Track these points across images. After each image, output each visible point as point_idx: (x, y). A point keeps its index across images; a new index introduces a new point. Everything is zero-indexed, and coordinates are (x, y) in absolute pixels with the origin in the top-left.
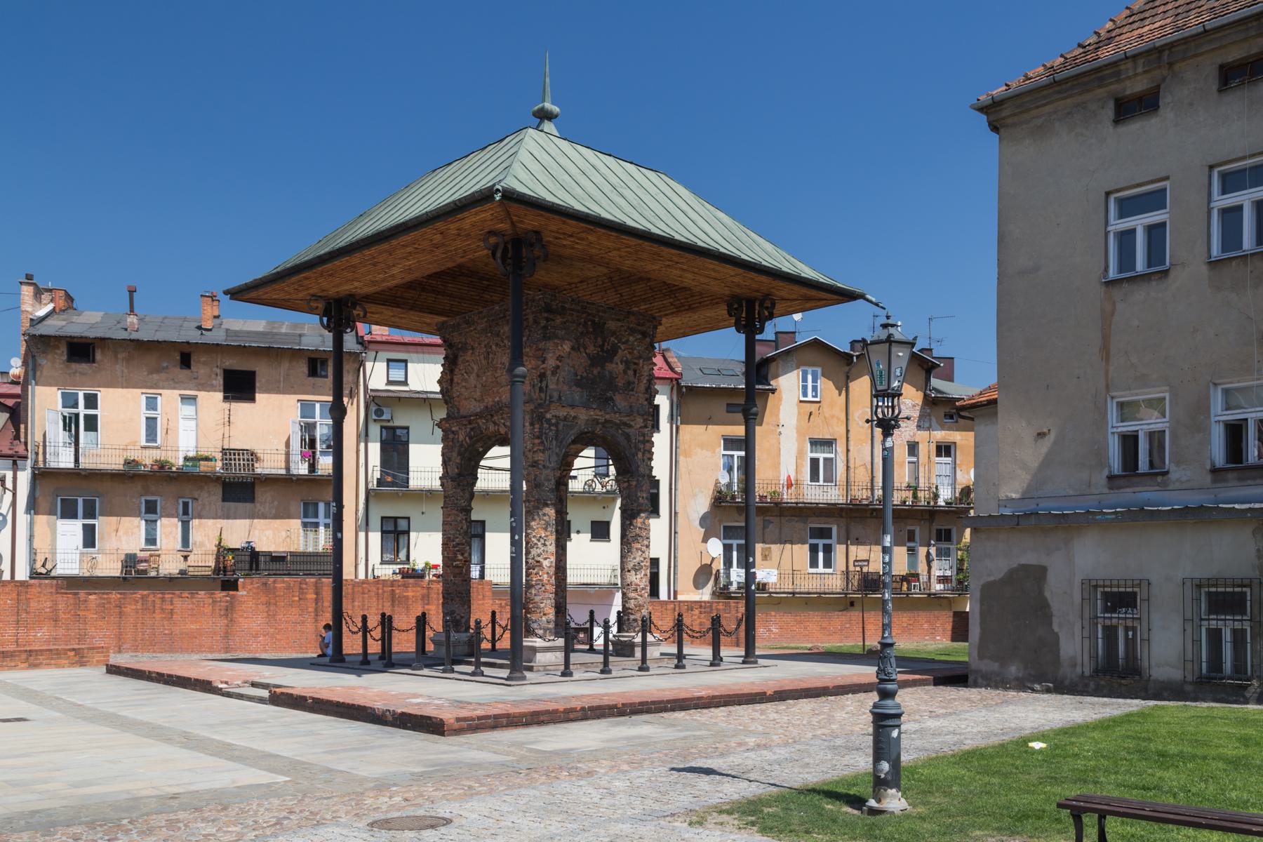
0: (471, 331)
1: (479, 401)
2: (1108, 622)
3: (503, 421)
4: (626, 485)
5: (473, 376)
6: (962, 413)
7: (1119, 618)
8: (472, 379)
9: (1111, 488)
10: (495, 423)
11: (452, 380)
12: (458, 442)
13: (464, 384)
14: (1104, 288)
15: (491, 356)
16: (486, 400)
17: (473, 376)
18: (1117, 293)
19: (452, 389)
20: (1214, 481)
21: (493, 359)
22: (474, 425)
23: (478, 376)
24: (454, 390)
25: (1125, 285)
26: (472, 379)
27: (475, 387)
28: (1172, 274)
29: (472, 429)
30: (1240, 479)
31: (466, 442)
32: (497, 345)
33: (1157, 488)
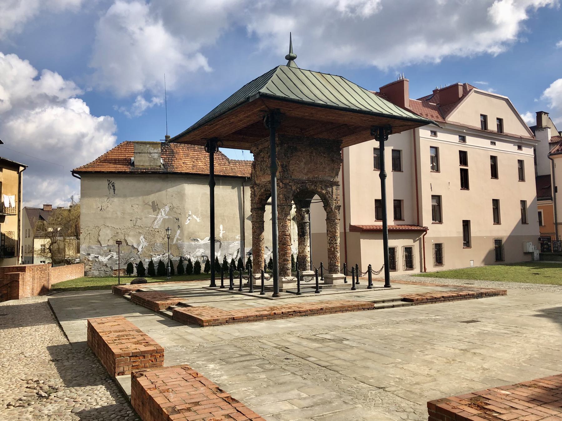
0: (300, 143)
1: (305, 175)
5: (302, 164)
6: (75, 174)
8: (302, 165)
10: (315, 186)
12: (292, 190)
13: (297, 165)
17: (302, 164)
22: (303, 185)
23: (305, 164)
24: (290, 167)
26: (302, 165)
27: (304, 168)
31: (297, 191)
32: (316, 153)
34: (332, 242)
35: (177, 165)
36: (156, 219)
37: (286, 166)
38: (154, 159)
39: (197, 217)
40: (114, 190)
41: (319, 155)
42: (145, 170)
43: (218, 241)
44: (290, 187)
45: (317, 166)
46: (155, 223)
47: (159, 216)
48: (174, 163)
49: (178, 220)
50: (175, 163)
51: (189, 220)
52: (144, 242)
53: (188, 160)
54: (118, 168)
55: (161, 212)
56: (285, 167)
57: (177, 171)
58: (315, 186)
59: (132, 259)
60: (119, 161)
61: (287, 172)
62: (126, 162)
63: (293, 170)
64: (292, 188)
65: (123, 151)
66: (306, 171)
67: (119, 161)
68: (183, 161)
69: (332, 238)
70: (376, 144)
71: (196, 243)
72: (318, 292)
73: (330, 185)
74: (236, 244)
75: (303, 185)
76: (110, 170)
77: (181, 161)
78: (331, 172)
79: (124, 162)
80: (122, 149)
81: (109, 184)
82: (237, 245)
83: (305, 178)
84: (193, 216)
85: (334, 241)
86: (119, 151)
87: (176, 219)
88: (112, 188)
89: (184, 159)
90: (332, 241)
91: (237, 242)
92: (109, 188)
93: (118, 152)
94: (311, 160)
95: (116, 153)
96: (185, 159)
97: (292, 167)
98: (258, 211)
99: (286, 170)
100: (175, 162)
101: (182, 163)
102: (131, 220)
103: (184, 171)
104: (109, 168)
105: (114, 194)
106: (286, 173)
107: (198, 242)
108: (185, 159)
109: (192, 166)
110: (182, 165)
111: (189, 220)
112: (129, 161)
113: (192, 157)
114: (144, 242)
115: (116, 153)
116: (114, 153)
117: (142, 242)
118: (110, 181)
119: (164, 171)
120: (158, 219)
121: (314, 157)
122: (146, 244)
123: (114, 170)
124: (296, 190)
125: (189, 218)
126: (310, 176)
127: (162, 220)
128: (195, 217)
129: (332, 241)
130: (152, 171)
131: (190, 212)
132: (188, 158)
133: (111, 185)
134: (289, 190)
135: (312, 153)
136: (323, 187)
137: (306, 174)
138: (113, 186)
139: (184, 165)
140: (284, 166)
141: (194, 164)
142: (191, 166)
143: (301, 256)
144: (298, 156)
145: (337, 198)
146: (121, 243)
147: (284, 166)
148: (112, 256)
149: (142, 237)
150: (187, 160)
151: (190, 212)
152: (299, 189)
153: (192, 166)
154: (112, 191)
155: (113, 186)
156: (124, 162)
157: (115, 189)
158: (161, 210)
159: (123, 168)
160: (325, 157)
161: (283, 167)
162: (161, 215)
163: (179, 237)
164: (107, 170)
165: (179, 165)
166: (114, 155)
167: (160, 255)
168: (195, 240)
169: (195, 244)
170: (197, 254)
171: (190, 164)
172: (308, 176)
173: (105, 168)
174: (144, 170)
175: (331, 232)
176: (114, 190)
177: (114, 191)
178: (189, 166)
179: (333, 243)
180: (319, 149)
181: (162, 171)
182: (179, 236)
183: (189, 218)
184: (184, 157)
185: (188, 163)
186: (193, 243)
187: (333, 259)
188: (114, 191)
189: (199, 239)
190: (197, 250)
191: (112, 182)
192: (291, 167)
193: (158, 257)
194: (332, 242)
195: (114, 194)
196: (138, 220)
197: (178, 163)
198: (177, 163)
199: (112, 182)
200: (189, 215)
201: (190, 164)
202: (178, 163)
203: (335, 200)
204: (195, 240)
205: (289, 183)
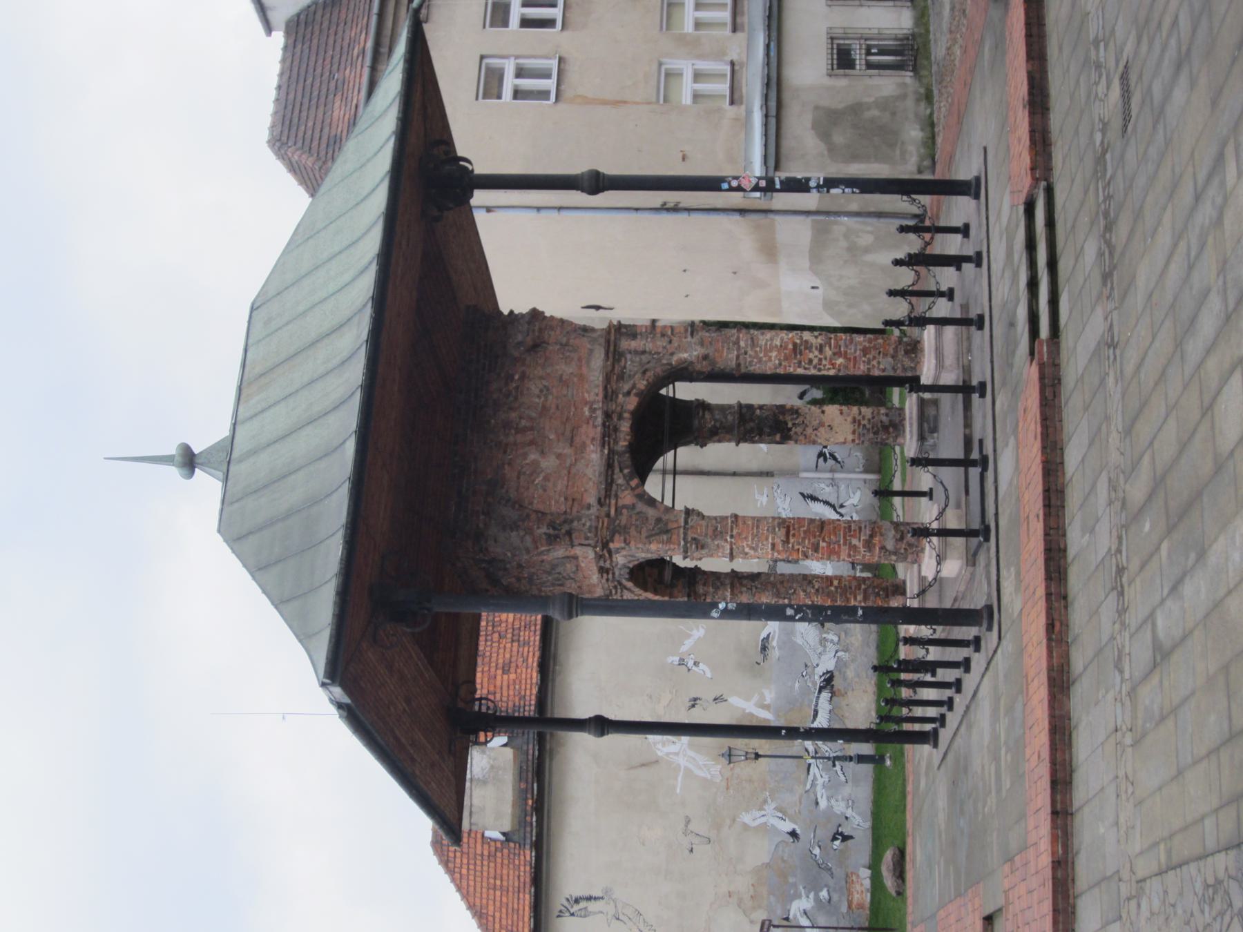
2: (864, 67)
3: (620, 396)
4: (708, 416)
7: (858, 56)
8: (549, 463)
9: (742, 103)
11: (537, 512)
12: (633, 506)
14: (561, 106)
15: (523, 423)
16: (584, 438)
18: (568, 92)
19: (552, 514)
20: (743, 30)
21: (531, 419)
24: (554, 509)
25: (563, 87)
26: (549, 463)
27: (559, 456)
28: (564, 55)
29: (621, 471)
30: (743, 14)
32: (511, 409)
33: (744, 69)
34: (815, 361)
35: (511, 693)
36: (688, 772)
37: (552, 525)
38: (492, 767)
39: (689, 636)
40: (589, 898)
41: (516, 398)
42: (526, 799)
43: (773, 568)
44: (625, 511)
45: (553, 406)
46: (701, 774)
47: (682, 761)
48: (504, 704)
49: (695, 699)
50: (505, 699)
51: (696, 664)
52: (763, 813)
53: (494, 655)
54: (522, 885)
55: (668, 754)
56: (554, 529)
57: (533, 697)
58: (620, 417)
59: (817, 851)
60: (498, 877)
61: (572, 521)
62: (499, 854)
63: (566, 499)
64: (624, 507)
65: (465, 861)
66: (568, 451)
67: (498, 877)
68: (500, 672)
69: (800, 362)
70: (480, 197)
71: (774, 643)
72: (982, 386)
73: (619, 360)
74: (786, 506)
75: (616, 464)
76: (527, 908)
77: (499, 678)
78: (575, 356)
79: (499, 860)
80: (458, 860)
81: (572, 915)
82: (788, 500)
83: (594, 457)
84: (684, 649)
85: (811, 356)
86: (464, 871)
87: (693, 706)
88: (583, 904)
89: (493, 670)
90: (810, 361)
91: (779, 501)
92: (585, 914)
93: (468, 875)
94: (532, 429)
95: (472, 883)
96: (493, 665)
97: (557, 502)
98: (695, 593)
99: (566, 528)
100: (501, 700)
101: (505, 677)
102: (691, 851)
103: (535, 675)
104: (521, 912)
105: (602, 898)
106: (575, 524)
107: (773, 638)
108: (493, 665)
109: (515, 644)
110: (513, 676)
111: (696, 664)
112: (499, 845)
113: (486, 641)
114: (763, 813)
115: (472, 883)
116: (471, 889)
117: (763, 820)
118: (561, 911)
119: (531, 740)
120: (691, 766)
121: (521, 418)
122: (770, 807)
123: (527, 896)
124: (633, 489)
125: (691, 663)
126: (591, 432)
127: (691, 753)
128: (687, 645)
129: (810, 361)
130: (530, 780)
131: (670, 659)
132: (488, 654)
133: (575, 908)
134: (634, 518)
135: (507, 425)
136: (626, 387)
137: (584, 445)
138: (577, 901)
139: (512, 670)
140: (551, 531)
141: (509, 636)
142: (515, 649)
143: (853, 441)
144: (518, 478)
145: (663, 335)
146: (767, 923)
147: (551, 531)
148: (805, 912)
149: (747, 818)
150: (494, 659)
151: (670, 659)
152: (631, 478)
153: (515, 644)
154: (593, 906)
155: (577, 901)
156: (499, 860)
157: (586, 894)
158: (659, 753)
159: (522, 868)
160: (523, 376)
161: (557, 537)
162: (677, 754)
163: (756, 698)
164: (526, 919)
165: (512, 687)
166: (478, 889)
167: (810, 765)
168: (764, 648)
169: (780, 648)
170: (812, 644)
171: (508, 650)
172: (588, 442)
173: (521, 924)
174: (526, 804)
175: (780, 364)
176: (589, 898)
177: (596, 899)
178: (515, 653)
179: (820, 360)
180: (495, 396)
181: (531, 746)
182: (748, 699)
183: (691, 663)
184: (486, 669)
185: (508, 656)
186: (775, 653)
187: (875, 363)
188: (596, 899)
189: (764, 635)
190: (799, 641)
191: (566, 903)
192: (556, 505)
193: (813, 769)
194: (815, 361)
195: (602, 898)
196: (691, 827)
197: (505, 688)
198: (505, 693)
199: (566, 903)
200: (682, 662)
201: (508, 650)
202: (505, 688)
203: (670, 342)
204: (764, 648)
205: (608, 515)
